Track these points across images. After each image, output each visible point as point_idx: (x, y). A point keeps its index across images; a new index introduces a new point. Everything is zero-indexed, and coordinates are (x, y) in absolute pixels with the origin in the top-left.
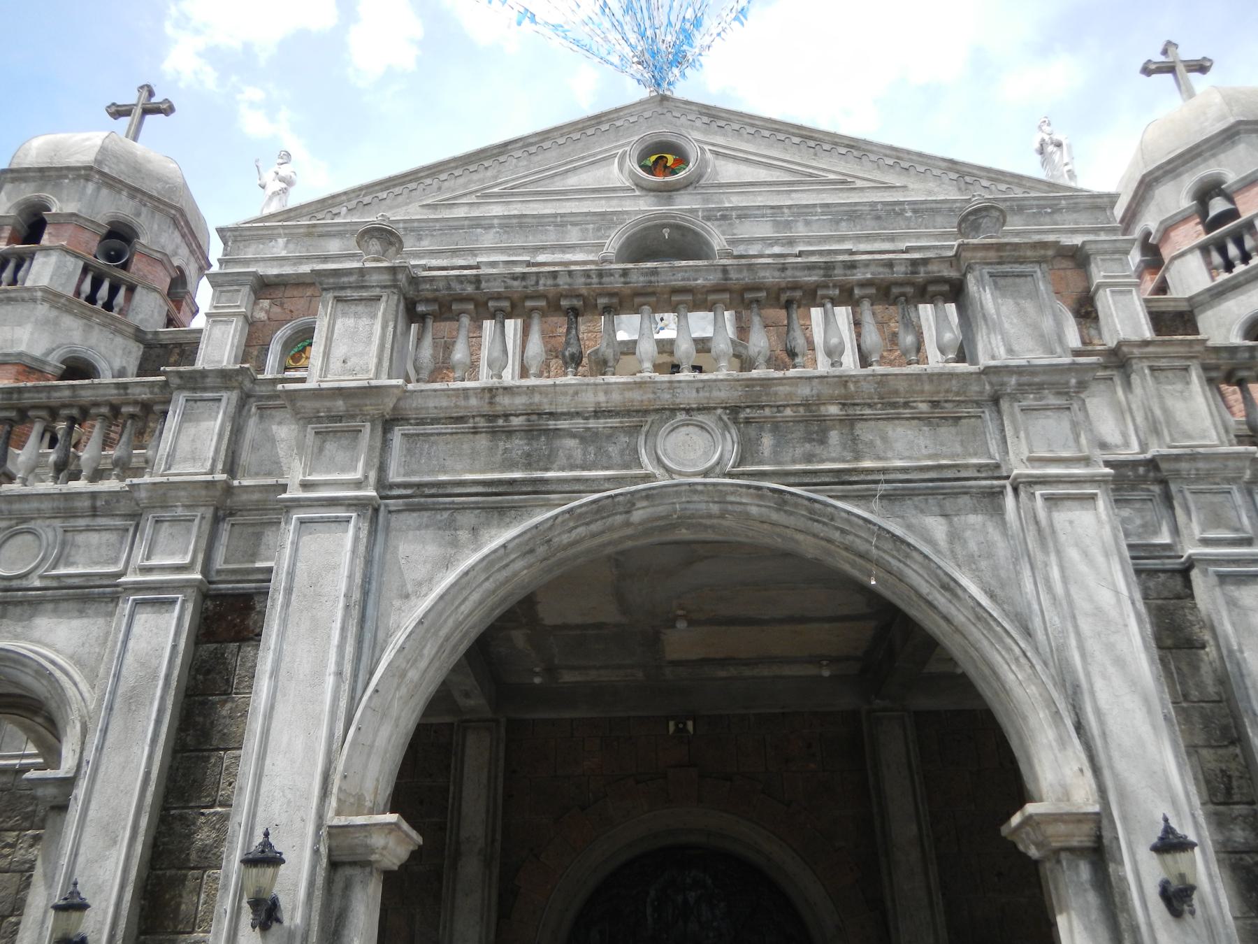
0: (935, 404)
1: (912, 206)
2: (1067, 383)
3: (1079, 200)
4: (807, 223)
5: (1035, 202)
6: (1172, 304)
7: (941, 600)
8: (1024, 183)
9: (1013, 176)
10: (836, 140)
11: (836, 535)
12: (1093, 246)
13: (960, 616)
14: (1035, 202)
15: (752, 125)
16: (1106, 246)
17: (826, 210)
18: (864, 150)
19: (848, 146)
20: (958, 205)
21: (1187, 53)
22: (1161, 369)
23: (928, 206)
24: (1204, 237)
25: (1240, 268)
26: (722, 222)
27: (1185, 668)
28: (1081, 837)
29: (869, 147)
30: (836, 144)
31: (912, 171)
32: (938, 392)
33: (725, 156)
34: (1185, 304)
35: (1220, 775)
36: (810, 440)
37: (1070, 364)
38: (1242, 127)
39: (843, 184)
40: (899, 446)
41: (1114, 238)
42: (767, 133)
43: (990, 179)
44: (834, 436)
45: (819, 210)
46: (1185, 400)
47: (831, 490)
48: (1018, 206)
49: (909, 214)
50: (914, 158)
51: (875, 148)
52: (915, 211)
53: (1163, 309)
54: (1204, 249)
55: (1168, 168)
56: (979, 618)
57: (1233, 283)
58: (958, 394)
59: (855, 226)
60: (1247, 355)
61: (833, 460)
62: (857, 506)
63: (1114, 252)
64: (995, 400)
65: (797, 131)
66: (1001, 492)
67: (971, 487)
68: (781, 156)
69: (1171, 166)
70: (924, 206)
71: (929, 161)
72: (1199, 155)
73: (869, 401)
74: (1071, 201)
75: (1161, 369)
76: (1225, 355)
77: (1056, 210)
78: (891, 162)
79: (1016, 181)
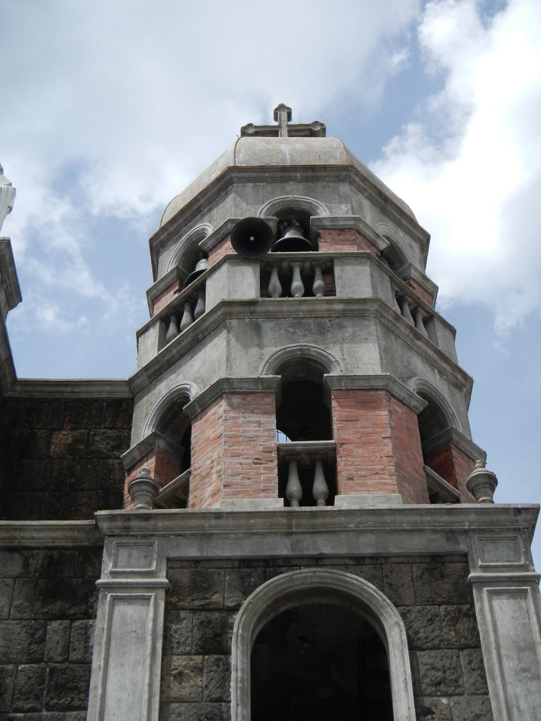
6: (108, 388)
34: (126, 389)
53: (95, 396)
55: (172, 229)
57: (167, 358)
69: (175, 226)
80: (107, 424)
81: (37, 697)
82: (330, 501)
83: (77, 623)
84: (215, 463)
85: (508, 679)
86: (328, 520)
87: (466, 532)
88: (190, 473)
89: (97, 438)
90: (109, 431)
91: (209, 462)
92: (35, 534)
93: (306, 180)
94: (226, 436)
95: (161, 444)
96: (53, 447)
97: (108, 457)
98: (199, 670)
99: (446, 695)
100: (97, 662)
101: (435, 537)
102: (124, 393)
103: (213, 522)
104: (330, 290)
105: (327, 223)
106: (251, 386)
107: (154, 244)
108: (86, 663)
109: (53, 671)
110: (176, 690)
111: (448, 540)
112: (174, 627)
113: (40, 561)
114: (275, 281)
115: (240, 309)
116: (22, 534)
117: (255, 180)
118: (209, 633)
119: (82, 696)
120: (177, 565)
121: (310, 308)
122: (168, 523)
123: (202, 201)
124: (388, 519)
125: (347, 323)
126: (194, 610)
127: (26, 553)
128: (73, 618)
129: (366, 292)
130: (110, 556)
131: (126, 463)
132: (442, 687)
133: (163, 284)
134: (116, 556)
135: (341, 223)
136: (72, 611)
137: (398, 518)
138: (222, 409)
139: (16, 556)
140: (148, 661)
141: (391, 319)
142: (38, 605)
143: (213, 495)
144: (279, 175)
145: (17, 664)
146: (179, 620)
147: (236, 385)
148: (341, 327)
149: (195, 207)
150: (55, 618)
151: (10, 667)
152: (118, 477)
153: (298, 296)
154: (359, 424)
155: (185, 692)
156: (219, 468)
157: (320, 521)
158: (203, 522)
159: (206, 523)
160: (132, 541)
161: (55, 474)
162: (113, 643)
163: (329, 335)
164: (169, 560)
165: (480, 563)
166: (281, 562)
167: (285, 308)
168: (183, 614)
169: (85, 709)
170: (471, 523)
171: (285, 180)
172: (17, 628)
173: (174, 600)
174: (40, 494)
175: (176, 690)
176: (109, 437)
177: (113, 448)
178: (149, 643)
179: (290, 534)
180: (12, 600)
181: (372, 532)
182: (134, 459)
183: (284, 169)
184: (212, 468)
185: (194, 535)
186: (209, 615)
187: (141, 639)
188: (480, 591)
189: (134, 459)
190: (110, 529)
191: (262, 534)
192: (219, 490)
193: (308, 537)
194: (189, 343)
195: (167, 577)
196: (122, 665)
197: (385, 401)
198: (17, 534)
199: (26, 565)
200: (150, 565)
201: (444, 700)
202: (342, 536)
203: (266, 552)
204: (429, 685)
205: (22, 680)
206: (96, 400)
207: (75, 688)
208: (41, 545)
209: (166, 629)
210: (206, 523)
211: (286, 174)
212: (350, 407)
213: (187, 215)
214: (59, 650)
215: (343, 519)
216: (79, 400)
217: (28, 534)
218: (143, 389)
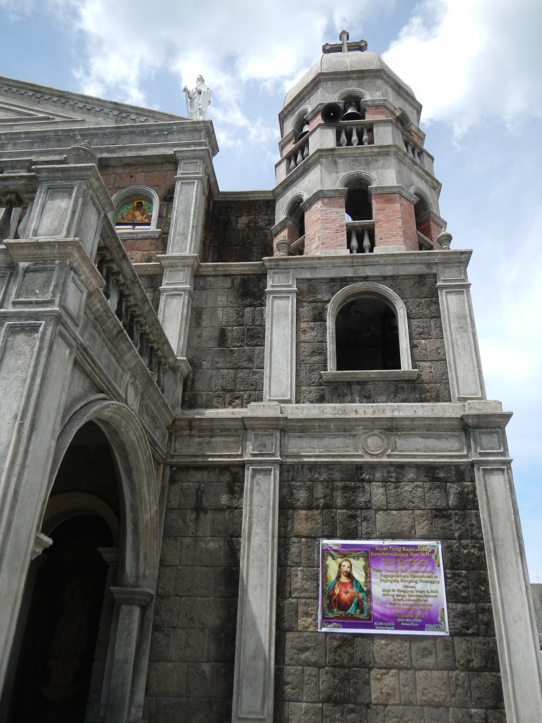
1: (80, 133)
3: (184, 126)
5: (156, 128)
6: (263, 195)
8: (156, 116)
10: (53, 92)
14: (156, 128)
15: (8, 85)
16: (188, 154)
17: (27, 136)
18: (68, 98)
19: (59, 96)
20: (109, 131)
21: (354, 38)
29: (70, 97)
30: (53, 95)
31: (93, 111)
34: (271, 195)
38: (321, 77)
39: (47, 120)
43: (137, 114)
45: (23, 136)
48: (146, 130)
49: (79, 137)
50: (95, 102)
51: (73, 97)
52: (82, 135)
55: (290, 108)
57: (291, 179)
59: (43, 146)
63: (194, 158)
65: (31, 88)
69: (291, 107)
70: (87, 132)
71: (103, 104)
72: (303, 98)
74: (180, 126)
78: (81, 105)
79: (152, 115)
80: (263, 213)
81: (242, 341)
82: (371, 250)
83: (257, 308)
84: (317, 233)
85: (453, 332)
86: (371, 259)
87: (436, 263)
88: (305, 237)
89: (259, 220)
90: (264, 216)
91: (314, 232)
92: (236, 269)
93: (358, 78)
94: (322, 219)
95: (290, 223)
96: (239, 225)
97: (265, 229)
98: (312, 329)
99: (424, 339)
100: (268, 326)
101: (421, 266)
102: (270, 197)
103: (317, 261)
104: (371, 141)
105: (369, 103)
106: (333, 193)
107: (281, 117)
108: (263, 326)
109: (248, 329)
110: (303, 337)
111: (427, 267)
112: (301, 310)
113: (239, 281)
114: (343, 137)
115: (326, 153)
116: (230, 269)
117: (332, 80)
118: (317, 312)
119: (262, 340)
120: (301, 281)
121: (361, 151)
122: (297, 262)
123: (305, 92)
124: (399, 258)
125: (380, 158)
126: (309, 302)
127: (232, 277)
128: (255, 306)
129: (389, 141)
130: (270, 277)
131: (274, 232)
132: (422, 335)
133: (287, 139)
134: (273, 278)
135: (377, 103)
136: (255, 303)
137: (404, 258)
138: (319, 206)
139: (228, 278)
140: (290, 325)
141: (402, 155)
142: (240, 300)
143: (316, 248)
144: (344, 76)
145: (232, 327)
146: (303, 307)
147: (326, 193)
148: (377, 161)
149: (301, 96)
150: (248, 306)
151: (230, 328)
152: (270, 239)
153: (355, 145)
154: (386, 211)
155: (307, 338)
156: (318, 235)
157: (367, 260)
158: (312, 261)
159: (314, 262)
160: (280, 271)
161: (241, 238)
162: (274, 317)
163: (371, 165)
164: (297, 279)
165: (442, 278)
166: (348, 280)
167: (349, 152)
168: (304, 304)
169: (264, 346)
170: (439, 259)
171: (348, 79)
172: (231, 311)
173: (300, 297)
174: (235, 248)
175: (303, 337)
176: (265, 220)
177: (267, 225)
178: (290, 317)
179: (353, 266)
180: (228, 298)
181: (391, 264)
182: (277, 230)
183: (347, 73)
184: (315, 235)
185: (308, 268)
186: (316, 304)
187: (287, 315)
188: (442, 292)
189: (277, 230)
190: (270, 266)
191: (340, 267)
192: (319, 246)
193: (361, 267)
194: (301, 171)
195: (297, 287)
196: (279, 327)
197: (398, 199)
198: (227, 268)
199: (233, 283)
200: (289, 282)
201: (423, 341)
202: (377, 267)
203: (342, 275)
204: (416, 335)
205: (235, 333)
206: (258, 201)
207: (259, 337)
208: (239, 273)
209: (297, 311)
210: (314, 262)
211: (348, 76)
212: (381, 203)
213: (297, 100)
214: (250, 321)
215: (378, 259)
216: (249, 201)
217: (233, 269)
218: (279, 195)
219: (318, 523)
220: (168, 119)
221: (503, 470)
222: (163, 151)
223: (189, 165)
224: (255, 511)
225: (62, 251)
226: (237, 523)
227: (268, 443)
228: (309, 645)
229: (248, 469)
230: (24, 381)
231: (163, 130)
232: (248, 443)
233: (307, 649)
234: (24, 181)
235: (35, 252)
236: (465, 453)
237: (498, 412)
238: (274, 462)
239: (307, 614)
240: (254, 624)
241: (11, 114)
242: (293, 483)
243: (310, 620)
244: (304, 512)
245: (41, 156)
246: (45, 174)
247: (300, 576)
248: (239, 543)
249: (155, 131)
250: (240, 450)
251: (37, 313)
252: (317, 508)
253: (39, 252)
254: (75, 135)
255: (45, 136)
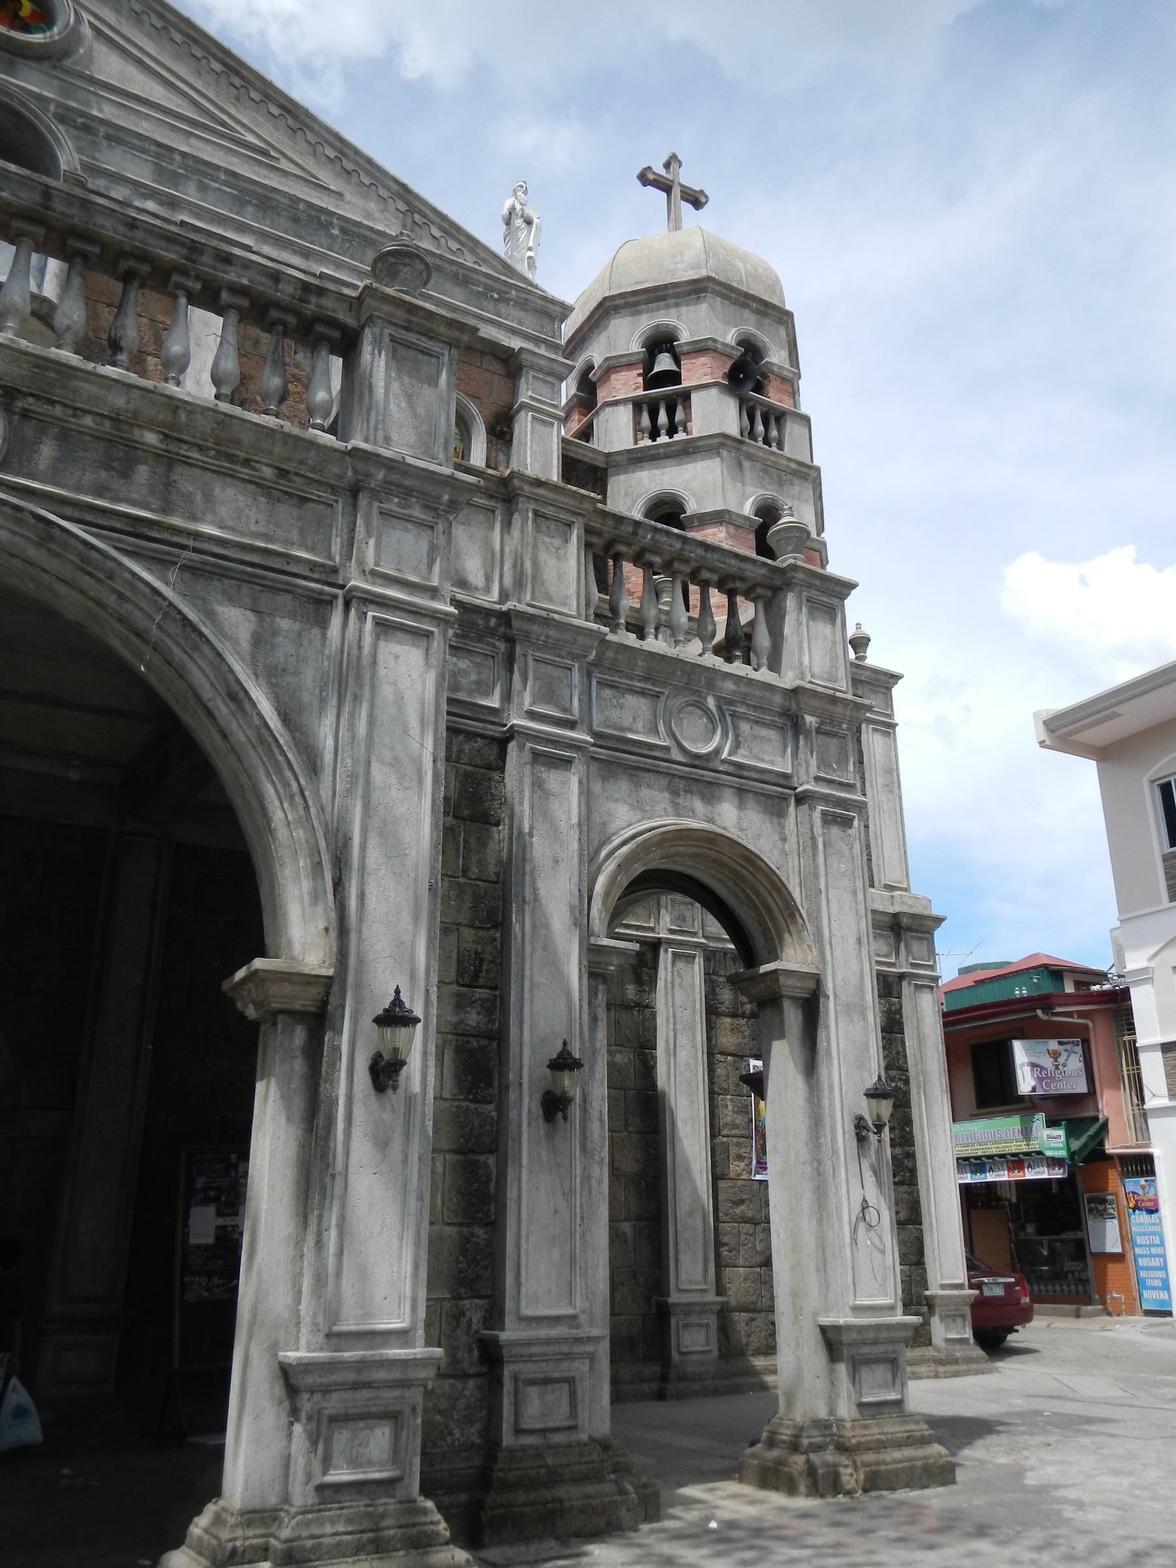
0: (283, 473)
1: (343, 224)
2: (439, 497)
3: (530, 297)
4: (203, 188)
5: (483, 280)
6: (590, 454)
7: (223, 709)
8: (479, 250)
9: (469, 237)
10: (271, 92)
11: (111, 599)
12: (529, 357)
13: (240, 734)
14: (483, 280)
16: (542, 362)
17: (232, 180)
18: (302, 122)
19: (281, 107)
21: (687, 177)
22: (545, 517)
23: (362, 231)
24: (640, 392)
25: (663, 439)
26: (82, 134)
27: (473, 842)
28: (304, 1000)
29: (309, 121)
31: (354, 178)
32: (289, 460)
33: (109, 40)
35: (473, 956)
36: (109, 468)
37: (449, 477)
38: (710, 285)
39: (263, 155)
40: (224, 511)
41: (554, 356)
42: (178, 38)
43: (442, 229)
44: (142, 473)
45: (223, 177)
46: (558, 558)
47: (120, 541)
48: (464, 276)
49: (336, 232)
51: (316, 127)
52: (344, 231)
54: (637, 405)
55: (632, 299)
56: (262, 741)
57: (653, 452)
58: (312, 469)
59: (264, 218)
60: (631, 529)
61: (134, 503)
62: (150, 571)
63: (549, 374)
64: (354, 492)
66: (330, 602)
67: (297, 586)
68: (191, 80)
70: (356, 230)
72: (664, 298)
73: (201, 442)
74: (523, 296)
75: (545, 517)
76: (611, 522)
77: (504, 299)
78: (332, 154)
79: (471, 245)
93: (757, 312)
104: (780, 446)
105: (775, 369)
107: (608, 304)
117: (724, 297)
123: (671, 291)
133: (625, 359)
135: (785, 373)
149: (661, 293)
167: (761, 454)
171: (744, 306)
183: (747, 295)
188: (867, 727)
213: (651, 295)
219: (745, 1037)
220: (501, 268)
221: (931, 988)
222: (498, 336)
223: (541, 384)
224: (679, 1015)
225: (855, 714)
226: (649, 1029)
227: (688, 914)
228: (744, 1197)
229: (666, 951)
230: (855, 893)
231: (493, 290)
232: (663, 911)
233: (742, 1202)
234: (763, 571)
235: (827, 707)
236: (893, 960)
237: (926, 912)
238: (697, 946)
239: (740, 1158)
240: (688, 1170)
241: (180, 102)
242: (715, 977)
243: (742, 1165)
244: (728, 1020)
245: (265, 242)
246: (801, 576)
247: (730, 1108)
248: (654, 1058)
249: (478, 284)
250: (652, 920)
251: (846, 800)
252: (743, 1016)
253: (831, 708)
254: (330, 225)
255: (269, 198)
